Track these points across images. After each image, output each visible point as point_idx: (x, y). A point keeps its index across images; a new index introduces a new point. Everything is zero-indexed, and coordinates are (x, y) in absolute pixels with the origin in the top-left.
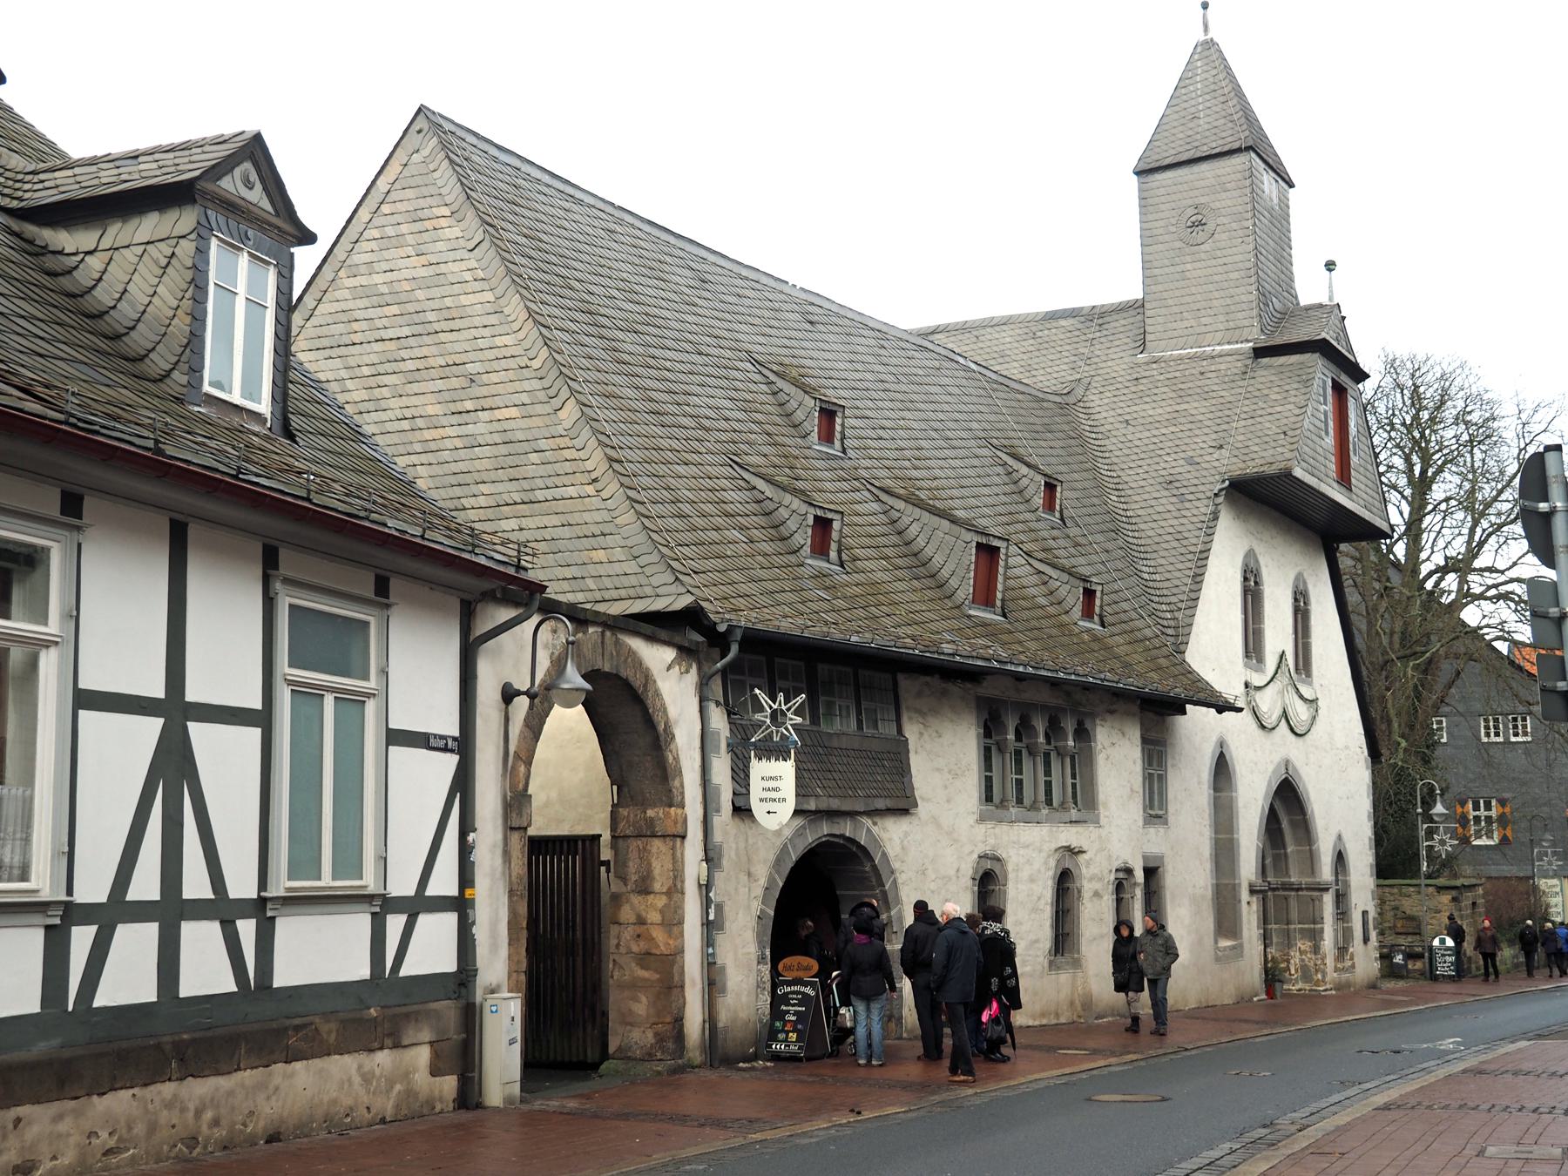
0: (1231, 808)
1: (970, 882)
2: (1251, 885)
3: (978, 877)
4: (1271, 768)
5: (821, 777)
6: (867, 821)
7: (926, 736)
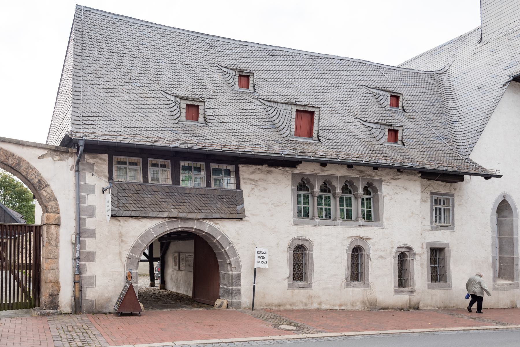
0: (512, 224)
1: (287, 249)
3: (293, 248)
5: (175, 204)
6: (207, 222)
7: (256, 189)
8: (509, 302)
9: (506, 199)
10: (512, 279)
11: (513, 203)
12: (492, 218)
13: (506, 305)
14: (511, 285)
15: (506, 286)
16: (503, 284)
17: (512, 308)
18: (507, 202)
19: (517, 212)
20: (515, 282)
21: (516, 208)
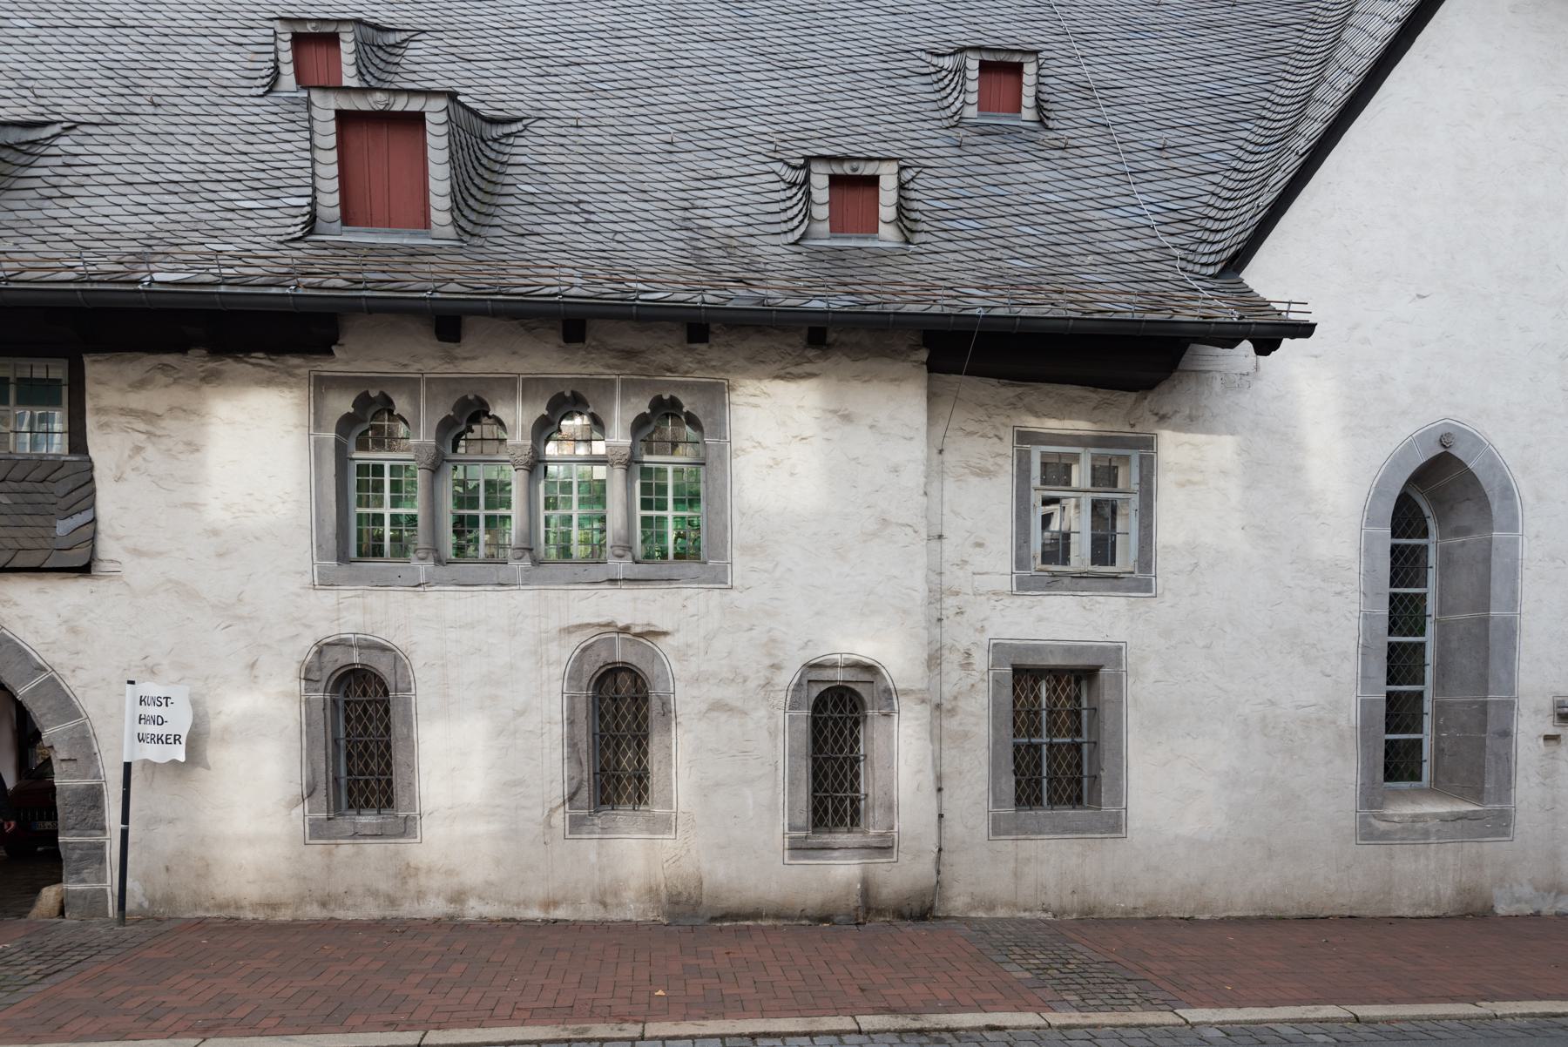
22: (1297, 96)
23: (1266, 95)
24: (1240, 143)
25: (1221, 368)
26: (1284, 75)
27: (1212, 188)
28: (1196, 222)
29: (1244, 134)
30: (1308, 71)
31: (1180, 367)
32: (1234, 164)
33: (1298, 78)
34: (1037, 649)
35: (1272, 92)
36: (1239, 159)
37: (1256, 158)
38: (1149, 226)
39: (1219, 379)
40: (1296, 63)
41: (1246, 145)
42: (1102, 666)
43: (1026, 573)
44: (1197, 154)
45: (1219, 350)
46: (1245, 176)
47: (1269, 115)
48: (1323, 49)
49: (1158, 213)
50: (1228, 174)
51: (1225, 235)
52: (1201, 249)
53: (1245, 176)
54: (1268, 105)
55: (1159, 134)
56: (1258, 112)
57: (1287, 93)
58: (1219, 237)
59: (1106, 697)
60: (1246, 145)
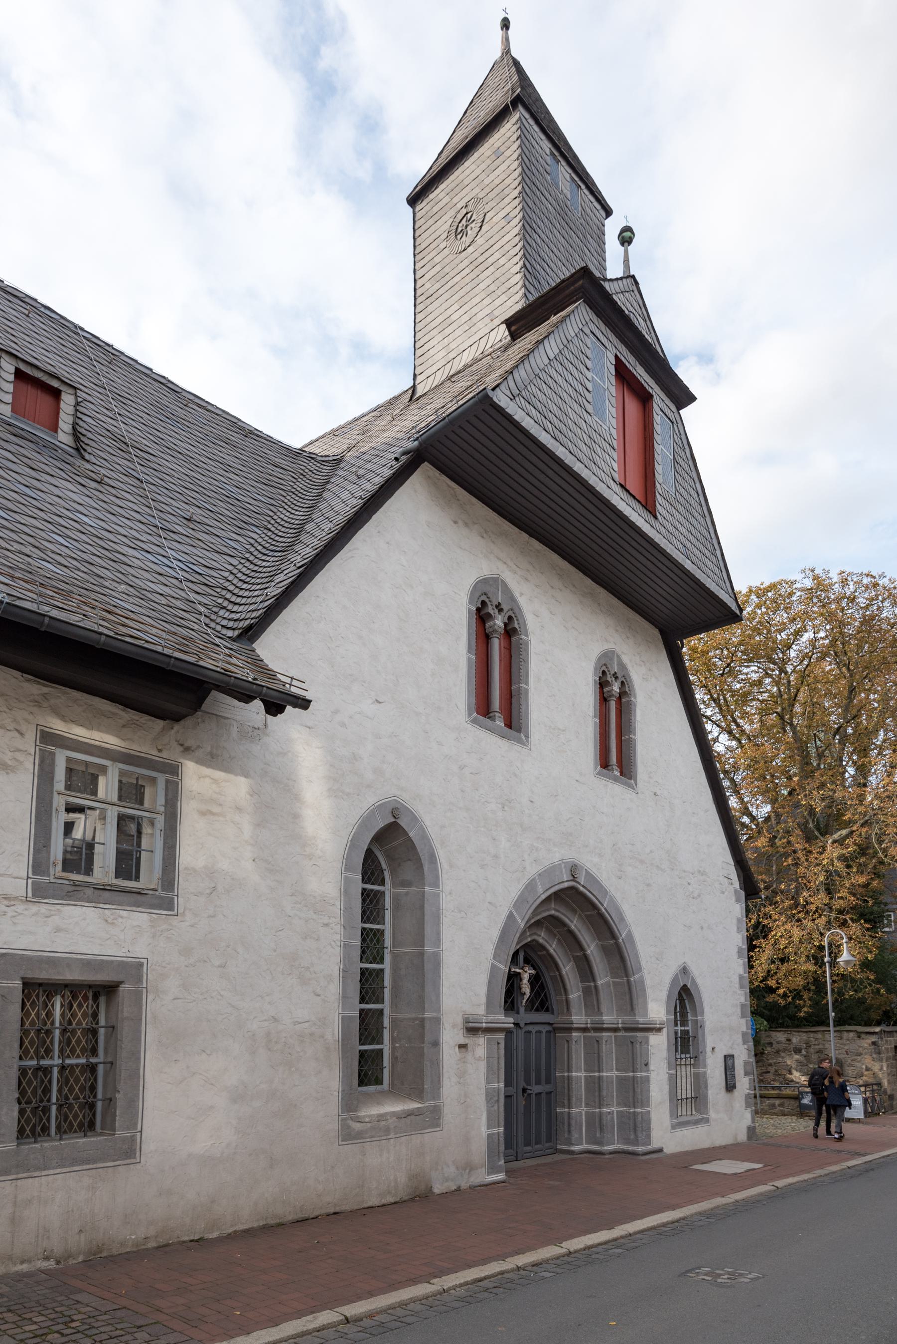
2: (467, 1021)
4: (533, 870)
8: (402, 1178)
9: (403, 823)
10: (418, 1093)
11: (425, 836)
12: (347, 881)
13: (389, 1193)
14: (412, 1117)
15: (392, 1121)
16: (381, 1117)
17: (412, 1200)
18: (405, 833)
19: (436, 869)
20: (427, 1104)
21: (433, 858)
22: (293, 524)
23: (271, 514)
24: (252, 541)
25: (238, 718)
26: (283, 504)
27: (230, 568)
28: (219, 590)
29: (255, 536)
30: (300, 509)
31: (204, 707)
32: (247, 555)
33: (293, 511)
34: (52, 962)
35: (275, 513)
36: (251, 553)
37: (264, 557)
38: (177, 579)
39: (235, 727)
40: (292, 500)
41: (256, 545)
42: (122, 982)
43: (45, 879)
44: (218, 536)
45: (236, 702)
46: (256, 568)
47: (273, 529)
48: (310, 498)
49: (185, 571)
50: (243, 561)
51: (241, 608)
52: (222, 613)
53: (256, 568)
54: (273, 522)
55: (187, 507)
56: (266, 524)
57: (285, 518)
58: (235, 608)
59: (126, 1014)
60: (256, 545)
